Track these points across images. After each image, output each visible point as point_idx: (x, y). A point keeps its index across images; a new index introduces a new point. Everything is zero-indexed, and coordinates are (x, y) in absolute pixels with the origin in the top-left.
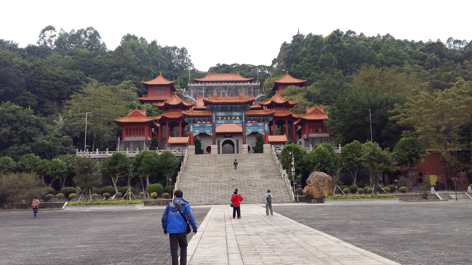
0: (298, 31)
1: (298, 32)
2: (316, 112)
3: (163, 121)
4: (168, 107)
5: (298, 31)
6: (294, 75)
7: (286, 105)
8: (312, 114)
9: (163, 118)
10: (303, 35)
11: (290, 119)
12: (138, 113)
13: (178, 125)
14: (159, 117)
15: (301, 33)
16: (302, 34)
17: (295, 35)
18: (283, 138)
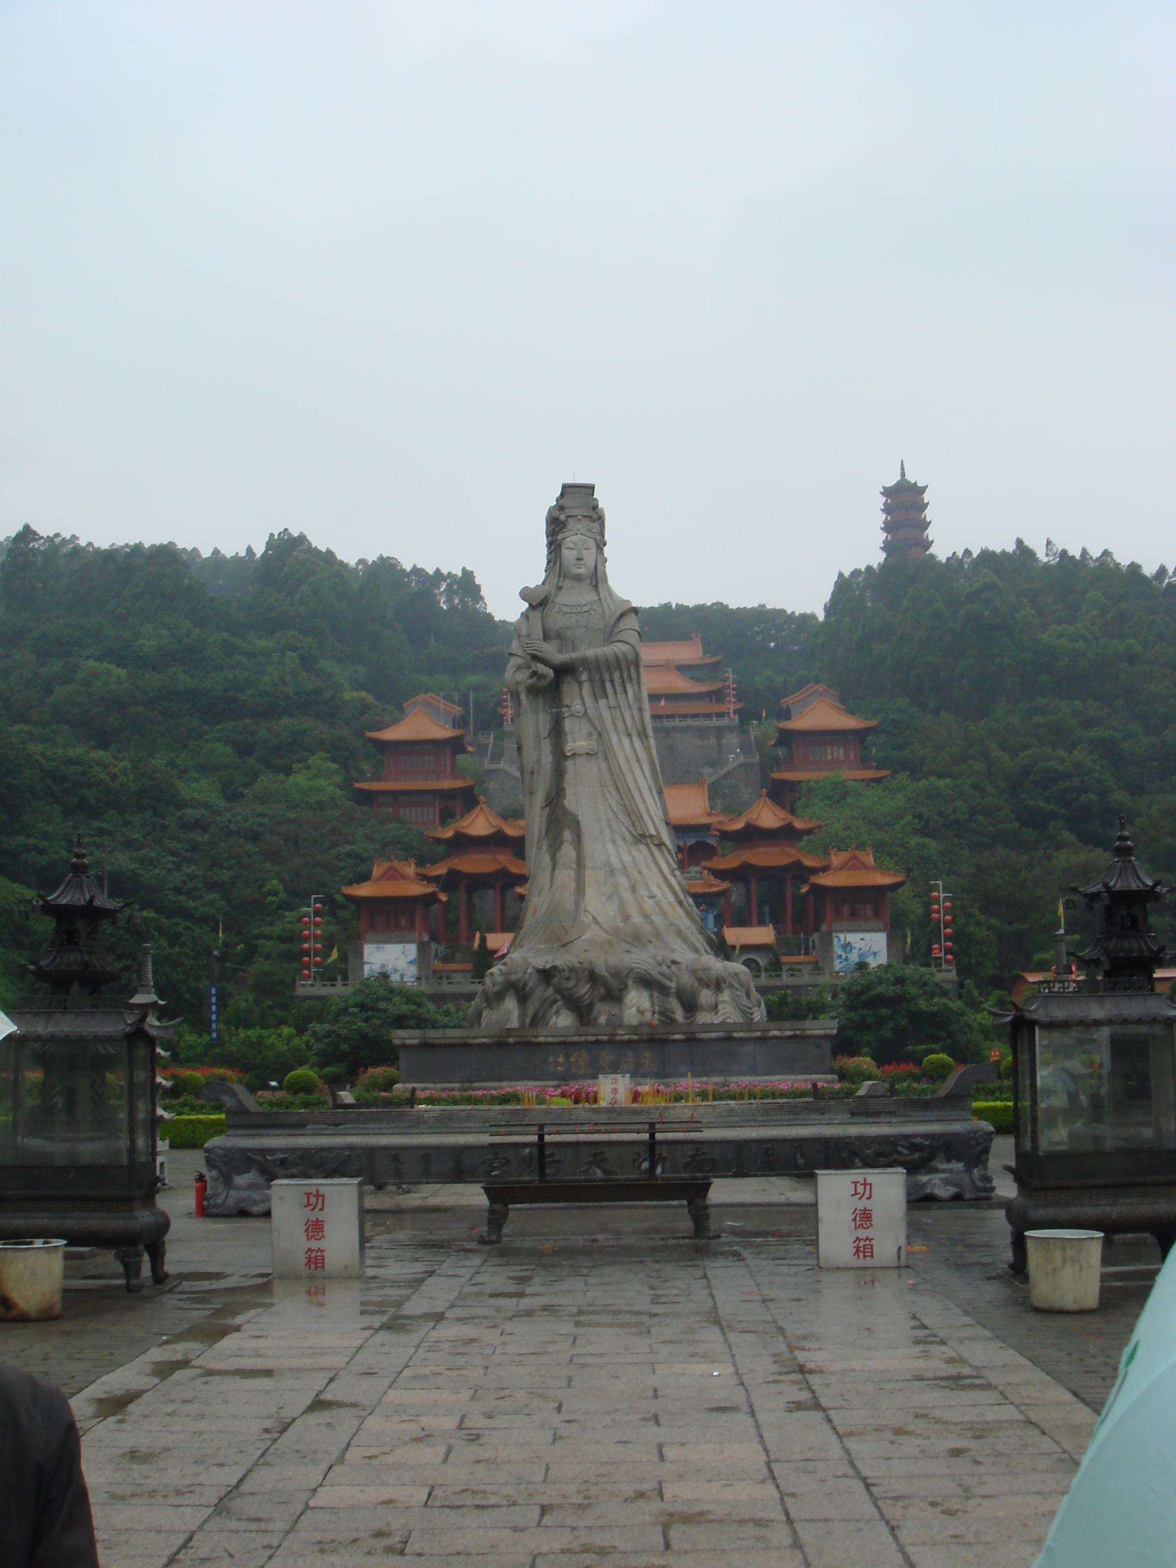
0: (903, 469)
1: (903, 474)
2: (854, 864)
3: (451, 881)
4: (462, 843)
5: (903, 469)
6: (847, 699)
7: (787, 834)
8: (841, 869)
10: (919, 484)
11: (800, 872)
12: (395, 870)
13: (492, 887)
14: (441, 870)
15: (911, 478)
16: (916, 483)
18: (763, 935)
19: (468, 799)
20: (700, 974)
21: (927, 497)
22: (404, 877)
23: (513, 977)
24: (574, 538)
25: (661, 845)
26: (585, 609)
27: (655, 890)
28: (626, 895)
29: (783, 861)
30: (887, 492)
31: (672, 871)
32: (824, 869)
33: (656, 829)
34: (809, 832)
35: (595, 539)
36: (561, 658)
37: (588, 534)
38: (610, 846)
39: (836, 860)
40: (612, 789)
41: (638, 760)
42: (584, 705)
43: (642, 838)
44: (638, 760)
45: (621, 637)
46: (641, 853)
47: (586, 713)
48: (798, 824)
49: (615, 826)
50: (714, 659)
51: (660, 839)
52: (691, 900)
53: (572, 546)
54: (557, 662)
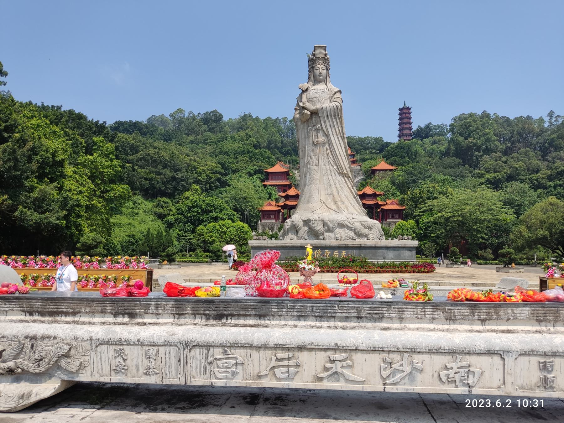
1: (405, 105)
3: (285, 207)
4: (287, 197)
7: (375, 196)
9: (285, 204)
11: (378, 206)
15: (407, 105)
17: (401, 107)
19: (289, 186)
20: (363, 223)
21: (411, 111)
22: (272, 205)
23: (294, 223)
24: (319, 66)
25: (348, 177)
26: (322, 91)
27: (346, 192)
28: (335, 193)
29: (373, 202)
30: (400, 110)
31: (352, 187)
32: (384, 205)
33: (347, 171)
34: (380, 195)
35: (326, 66)
36: (313, 108)
37: (323, 64)
38: (330, 177)
39: (389, 202)
40: (331, 156)
41: (341, 146)
42: (321, 125)
43: (343, 174)
44: (341, 146)
45: (335, 100)
46: (341, 179)
47: (322, 128)
48: (377, 193)
49: (332, 169)
50: (354, 153)
51: (348, 174)
52: (358, 197)
53: (318, 68)
54: (312, 109)
